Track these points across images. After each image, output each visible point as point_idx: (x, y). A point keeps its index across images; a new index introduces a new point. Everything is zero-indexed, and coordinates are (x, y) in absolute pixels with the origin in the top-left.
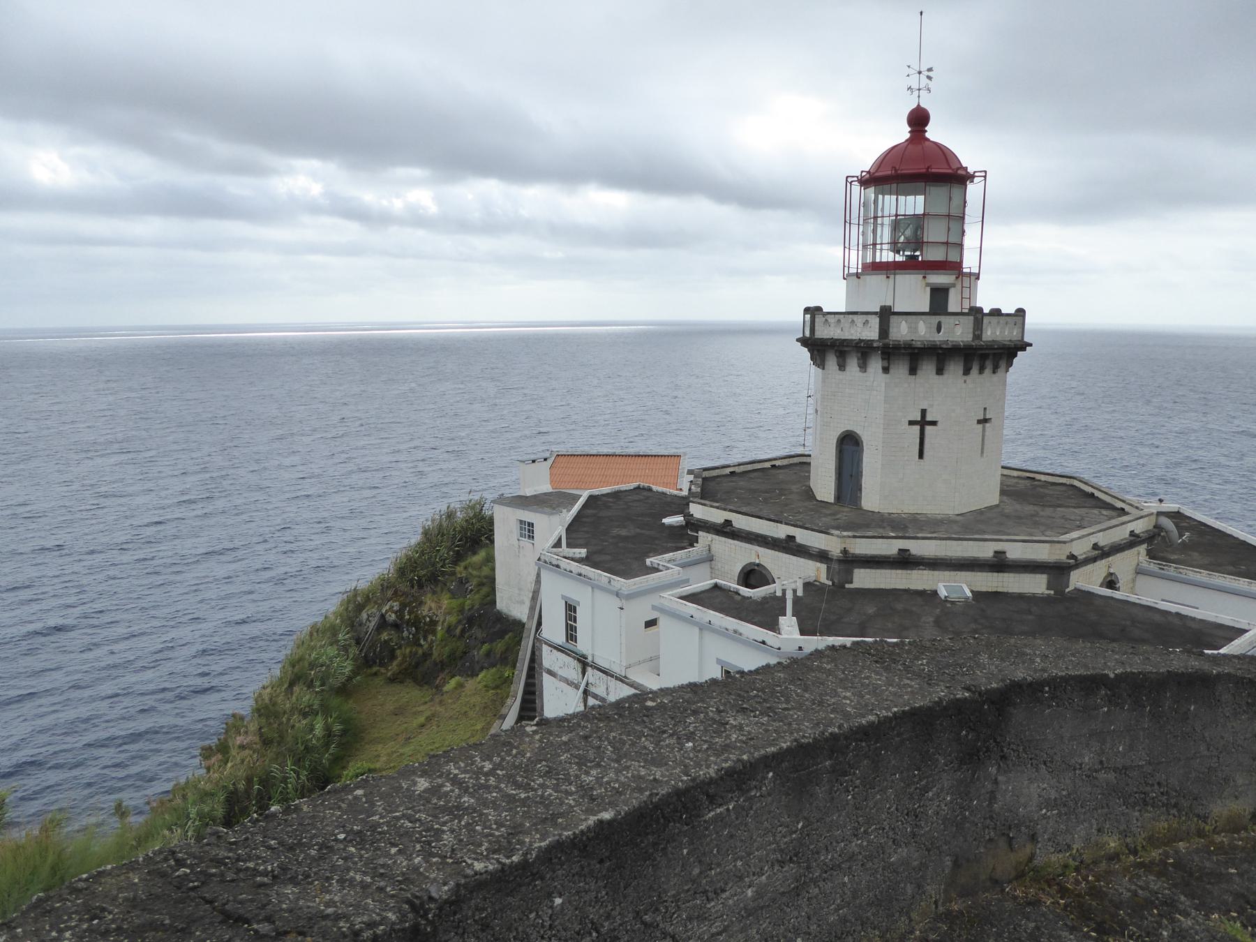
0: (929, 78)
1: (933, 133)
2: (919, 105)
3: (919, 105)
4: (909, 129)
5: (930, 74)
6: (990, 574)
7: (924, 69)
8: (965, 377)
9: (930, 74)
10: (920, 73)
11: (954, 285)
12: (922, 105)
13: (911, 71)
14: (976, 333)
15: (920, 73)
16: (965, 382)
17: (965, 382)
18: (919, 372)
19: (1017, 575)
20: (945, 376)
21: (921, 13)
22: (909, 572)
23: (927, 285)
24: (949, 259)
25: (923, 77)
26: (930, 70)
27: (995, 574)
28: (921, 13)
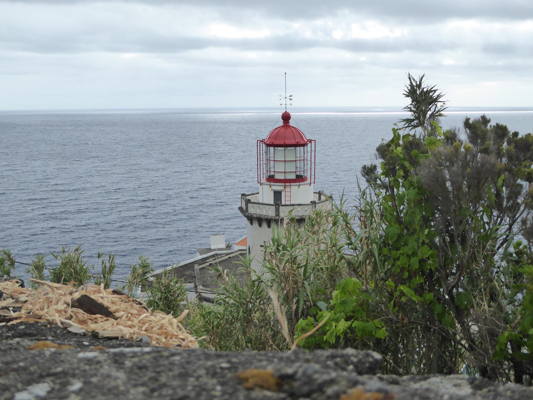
0: (291, 99)
2: (286, 111)
3: (286, 111)
4: (283, 121)
5: (291, 98)
7: (288, 96)
9: (291, 98)
10: (286, 98)
11: (283, 190)
13: (281, 98)
15: (286, 98)
18: (262, 226)
23: (272, 190)
24: (286, 178)
25: (288, 99)
26: (291, 96)
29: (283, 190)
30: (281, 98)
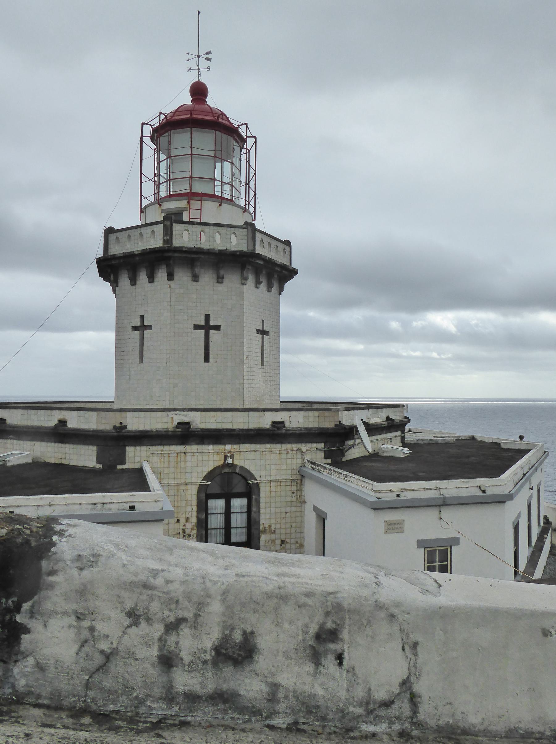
0: (208, 59)
1: (212, 101)
5: (209, 56)
6: (56, 445)
8: (170, 282)
9: (209, 56)
10: (199, 57)
12: (202, 80)
13: (189, 57)
14: (165, 238)
15: (199, 57)
16: (170, 286)
17: (170, 286)
19: (75, 446)
20: (156, 283)
21: (199, 13)
22: (5, 441)
25: (202, 60)
27: (60, 445)
28: (199, 13)
29: (185, 209)
30: (189, 57)
